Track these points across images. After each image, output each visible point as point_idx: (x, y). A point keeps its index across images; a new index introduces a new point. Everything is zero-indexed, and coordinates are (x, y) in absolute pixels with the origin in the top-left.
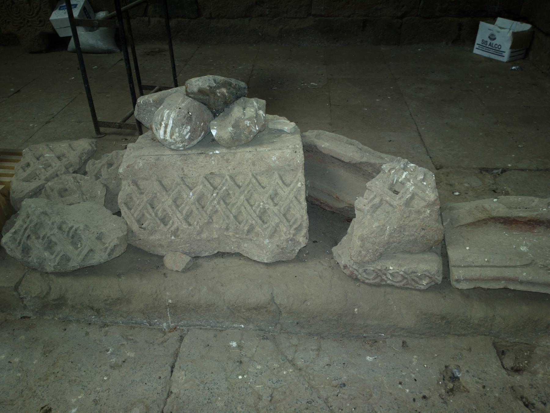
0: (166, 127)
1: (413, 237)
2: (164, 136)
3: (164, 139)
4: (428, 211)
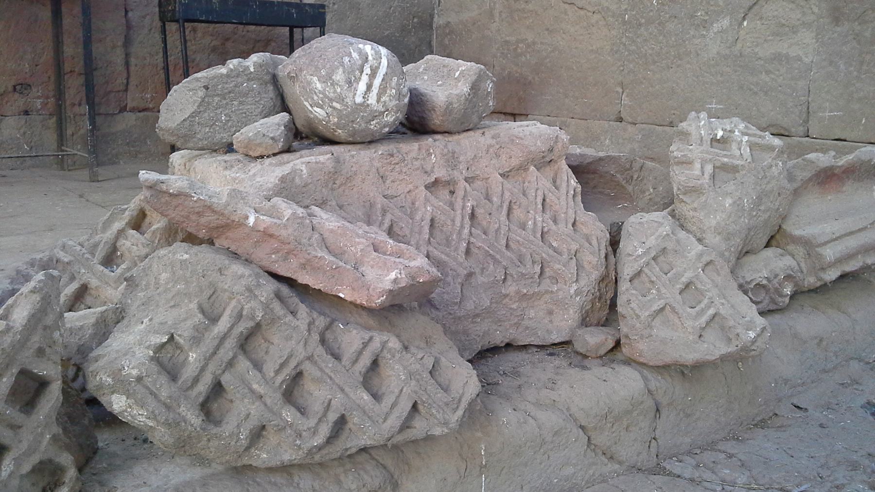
1: (768, 214)
3: (361, 105)
4: (780, 163)
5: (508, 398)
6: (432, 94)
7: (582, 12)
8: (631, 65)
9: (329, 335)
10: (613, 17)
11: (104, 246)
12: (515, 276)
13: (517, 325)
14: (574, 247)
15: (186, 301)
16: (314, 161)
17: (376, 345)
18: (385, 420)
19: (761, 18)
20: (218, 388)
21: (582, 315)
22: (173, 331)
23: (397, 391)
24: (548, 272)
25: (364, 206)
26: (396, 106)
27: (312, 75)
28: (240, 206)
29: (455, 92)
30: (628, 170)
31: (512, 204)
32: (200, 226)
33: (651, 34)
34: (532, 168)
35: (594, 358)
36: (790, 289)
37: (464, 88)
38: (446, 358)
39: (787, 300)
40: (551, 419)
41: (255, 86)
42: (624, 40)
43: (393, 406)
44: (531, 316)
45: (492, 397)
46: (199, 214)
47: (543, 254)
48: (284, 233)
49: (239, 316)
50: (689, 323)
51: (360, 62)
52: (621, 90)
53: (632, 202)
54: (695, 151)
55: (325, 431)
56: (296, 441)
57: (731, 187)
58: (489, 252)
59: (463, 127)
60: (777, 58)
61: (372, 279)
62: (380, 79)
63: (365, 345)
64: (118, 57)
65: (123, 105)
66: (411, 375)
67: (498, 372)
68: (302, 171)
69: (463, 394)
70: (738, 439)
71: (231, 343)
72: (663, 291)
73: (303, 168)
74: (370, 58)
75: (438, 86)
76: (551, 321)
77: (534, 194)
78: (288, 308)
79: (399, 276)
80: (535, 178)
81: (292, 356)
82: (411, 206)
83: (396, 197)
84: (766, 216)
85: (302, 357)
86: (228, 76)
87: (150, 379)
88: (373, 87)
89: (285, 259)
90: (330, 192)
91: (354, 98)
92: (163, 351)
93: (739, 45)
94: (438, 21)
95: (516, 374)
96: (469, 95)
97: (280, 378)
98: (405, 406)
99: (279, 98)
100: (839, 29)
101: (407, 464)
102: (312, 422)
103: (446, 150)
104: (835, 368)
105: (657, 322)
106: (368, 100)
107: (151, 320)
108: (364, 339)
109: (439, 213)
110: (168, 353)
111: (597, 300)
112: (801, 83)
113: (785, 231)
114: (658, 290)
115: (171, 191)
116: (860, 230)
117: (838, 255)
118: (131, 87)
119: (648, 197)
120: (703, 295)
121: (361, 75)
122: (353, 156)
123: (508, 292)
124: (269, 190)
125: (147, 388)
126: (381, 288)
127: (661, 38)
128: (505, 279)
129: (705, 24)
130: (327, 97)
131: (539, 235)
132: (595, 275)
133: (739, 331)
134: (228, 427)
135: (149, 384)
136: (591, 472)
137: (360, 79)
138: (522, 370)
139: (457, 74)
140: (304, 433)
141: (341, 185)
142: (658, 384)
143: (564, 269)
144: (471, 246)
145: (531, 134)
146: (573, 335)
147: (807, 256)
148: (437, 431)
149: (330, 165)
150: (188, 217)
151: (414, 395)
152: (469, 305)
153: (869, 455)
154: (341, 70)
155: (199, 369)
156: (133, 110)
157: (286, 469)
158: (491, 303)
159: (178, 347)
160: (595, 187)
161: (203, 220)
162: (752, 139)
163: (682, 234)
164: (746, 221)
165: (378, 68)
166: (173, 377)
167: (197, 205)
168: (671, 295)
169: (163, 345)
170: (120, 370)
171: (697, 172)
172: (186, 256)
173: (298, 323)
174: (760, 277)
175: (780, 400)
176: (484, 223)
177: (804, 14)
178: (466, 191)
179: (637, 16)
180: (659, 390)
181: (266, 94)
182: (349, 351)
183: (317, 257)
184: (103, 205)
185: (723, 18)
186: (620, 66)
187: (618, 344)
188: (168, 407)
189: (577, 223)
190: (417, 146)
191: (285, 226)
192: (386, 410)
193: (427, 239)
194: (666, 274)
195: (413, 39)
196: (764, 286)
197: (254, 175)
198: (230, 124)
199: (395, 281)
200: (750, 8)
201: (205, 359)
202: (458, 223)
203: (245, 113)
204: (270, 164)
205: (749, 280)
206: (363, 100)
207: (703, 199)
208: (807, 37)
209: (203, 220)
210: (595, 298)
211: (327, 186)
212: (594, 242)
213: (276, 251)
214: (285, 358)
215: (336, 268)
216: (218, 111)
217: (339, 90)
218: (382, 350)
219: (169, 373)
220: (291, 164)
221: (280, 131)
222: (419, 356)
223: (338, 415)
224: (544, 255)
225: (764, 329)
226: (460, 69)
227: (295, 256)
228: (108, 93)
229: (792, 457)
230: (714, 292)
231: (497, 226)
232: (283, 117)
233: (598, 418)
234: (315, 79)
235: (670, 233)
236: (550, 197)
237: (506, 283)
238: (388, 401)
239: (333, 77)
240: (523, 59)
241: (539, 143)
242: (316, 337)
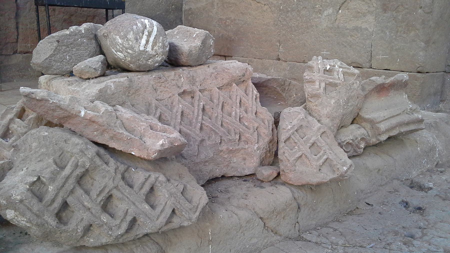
0: (149, 35)
2: (144, 47)
4: (358, 82)
5: (223, 204)
6: (181, 45)
7: (259, 4)
8: (284, 32)
9: (126, 175)
10: (274, 7)
11: (2, 128)
12: (226, 141)
13: (228, 166)
14: (256, 125)
15: (47, 158)
16: (118, 81)
17: (152, 179)
18: (157, 219)
19: (348, 9)
20: (65, 205)
21: (261, 160)
22: (39, 175)
23: (164, 203)
24: (243, 138)
25: (146, 105)
26: (162, 52)
27: (116, 35)
28: (76, 106)
29: (193, 45)
30: (282, 85)
31: (224, 103)
32: (54, 117)
33: (293, 16)
34: (234, 85)
35: (267, 182)
36: (363, 145)
37: (198, 43)
38: (190, 185)
39: (362, 150)
40: (244, 214)
41: (85, 41)
42: (280, 19)
43: (162, 211)
44: (234, 161)
45: (214, 204)
46: (54, 110)
47: (240, 129)
48: (100, 120)
49: (77, 166)
50: (314, 163)
51: (142, 29)
52: (279, 44)
53: (285, 102)
54: (316, 76)
55: (125, 226)
56: (109, 232)
57: (334, 94)
58: (212, 128)
59: (198, 63)
60: (356, 29)
61: (150, 144)
63: (146, 179)
64: (12, 24)
65: (15, 50)
66: (171, 194)
67: (218, 191)
68: (111, 86)
69: (199, 204)
70: (339, 221)
71: (72, 181)
72: (301, 147)
73: (112, 84)
74: (148, 26)
75: (184, 42)
76: (245, 164)
77: (235, 98)
78: (103, 161)
79: (164, 142)
80: (236, 90)
81: (106, 186)
82: (171, 104)
83: (163, 100)
84: (351, 108)
85: (111, 187)
86: (70, 35)
87: (27, 201)
88: (149, 42)
89: (102, 134)
90: (127, 98)
91: (139, 47)
92: (34, 185)
93: (337, 22)
94: (185, 7)
95: (227, 191)
96: (201, 46)
97: (100, 199)
98: (168, 211)
99: (98, 47)
100: (386, 15)
101: (170, 241)
102: (118, 222)
103: (189, 75)
104: (386, 184)
105: (298, 163)
106: (147, 49)
107: (27, 169)
108: (146, 176)
109: (186, 108)
110: (37, 186)
111: (268, 152)
112: (368, 42)
113: (361, 116)
114: (299, 147)
115: (37, 98)
116: (397, 115)
117: (387, 128)
118: (20, 40)
119: (293, 99)
120: (321, 149)
121: (143, 35)
122: (139, 78)
123: (222, 149)
124: (93, 97)
125: (26, 206)
126: (154, 149)
127: (298, 18)
128: (221, 142)
129: (320, 12)
130: (124, 47)
131: (238, 119)
132: (267, 139)
133: (338, 167)
134: (72, 226)
135: (27, 204)
136: (266, 241)
137: (142, 37)
138: (230, 189)
139: (194, 36)
140: (113, 228)
141: (133, 94)
142: (299, 195)
143: (251, 136)
144: (203, 126)
145: (233, 67)
146: (256, 170)
147: (372, 128)
148: (186, 224)
150: (47, 112)
151: (173, 205)
152: (202, 156)
153: (403, 227)
154: (132, 33)
155: (54, 195)
156: (21, 53)
157: (103, 247)
158: (214, 155)
159: (43, 183)
160: (266, 94)
161: (56, 114)
162: (344, 70)
163: (310, 118)
164: (342, 111)
165: (152, 32)
166: (40, 200)
167: (52, 106)
168: (305, 149)
169: (34, 183)
170: (11, 196)
171: (317, 87)
172: (46, 134)
173: (109, 169)
174: (349, 139)
175: (359, 201)
176: (210, 113)
177: (369, 7)
178: (200, 97)
179: (287, 7)
180: (300, 198)
181: (91, 45)
182: (137, 183)
183: (119, 133)
184: (5, 104)
185: (329, 8)
186: (278, 32)
187: (279, 174)
188: (38, 216)
189: (257, 113)
190: (174, 73)
191: (101, 116)
192: (158, 213)
193: (179, 122)
194: (302, 138)
195: (172, 16)
196: (351, 144)
197: (85, 89)
198: (71, 61)
199: (162, 145)
200: (343, 3)
201: (58, 189)
202: (196, 114)
203: (80, 55)
204: (94, 83)
205: (343, 141)
206: (144, 49)
207: (320, 100)
208: (371, 18)
209: (56, 114)
210: (267, 151)
211: (125, 94)
212: (266, 123)
213: (97, 130)
214: (102, 187)
215: (130, 139)
216: (65, 54)
217: (131, 43)
218: (156, 182)
219: (38, 197)
220: (105, 83)
221: (99, 65)
222: (176, 185)
223: (132, 217)
224: (241, 129)
225: (351, 166)
226: (196, 33)
227: (107, 132)
228: (7, 44)
229: (366, 230)
230: (327, 147)
231: (216, 115)
232: (100, 57)
233: (270, 213)
234: (118, 37)
235: (304, 117)
236: (244, 99)
237: (221, 144)
238: (159, 209)
239: (128, 36)
240: (229, 28)
241: (237, 72)
242: (120, 176)
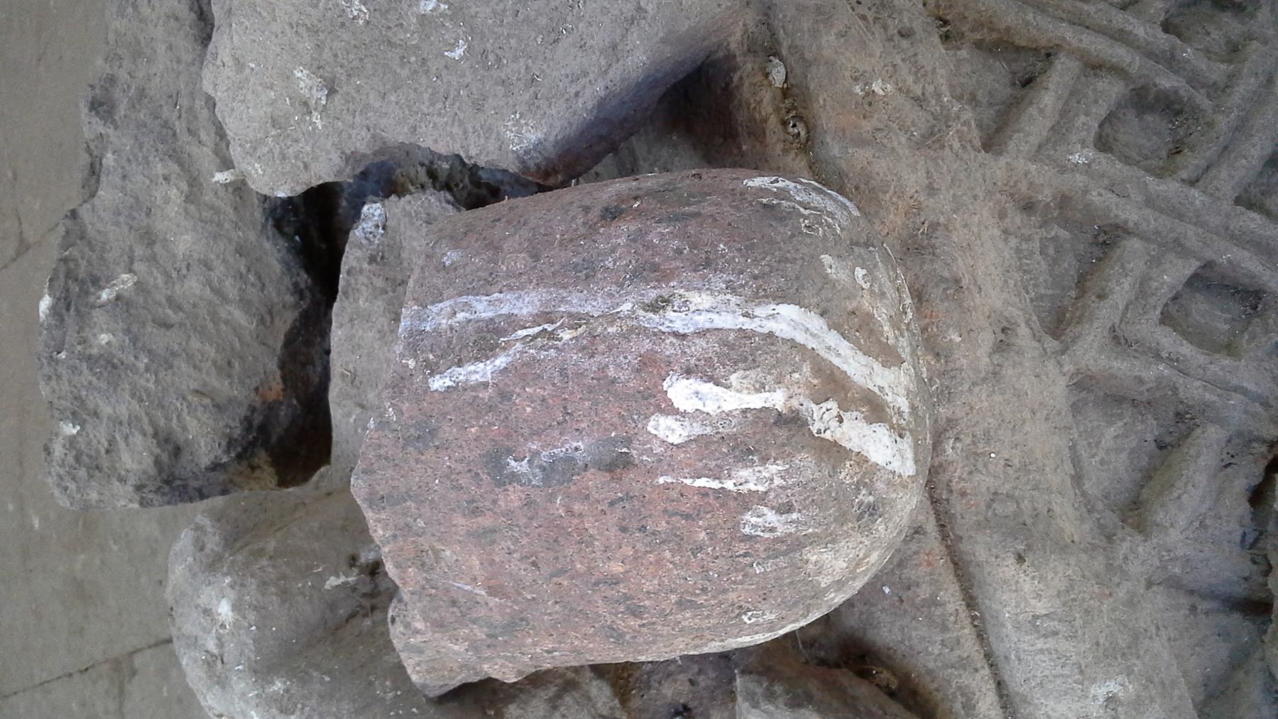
51: (805, 460)
62: (845, 347)
68: (1111, 699)
73: (1100, 691)
74: (777, 399)
122: (973, 455)
137: (862, 460)
149: (1059, 572)
206: (908, 439)
